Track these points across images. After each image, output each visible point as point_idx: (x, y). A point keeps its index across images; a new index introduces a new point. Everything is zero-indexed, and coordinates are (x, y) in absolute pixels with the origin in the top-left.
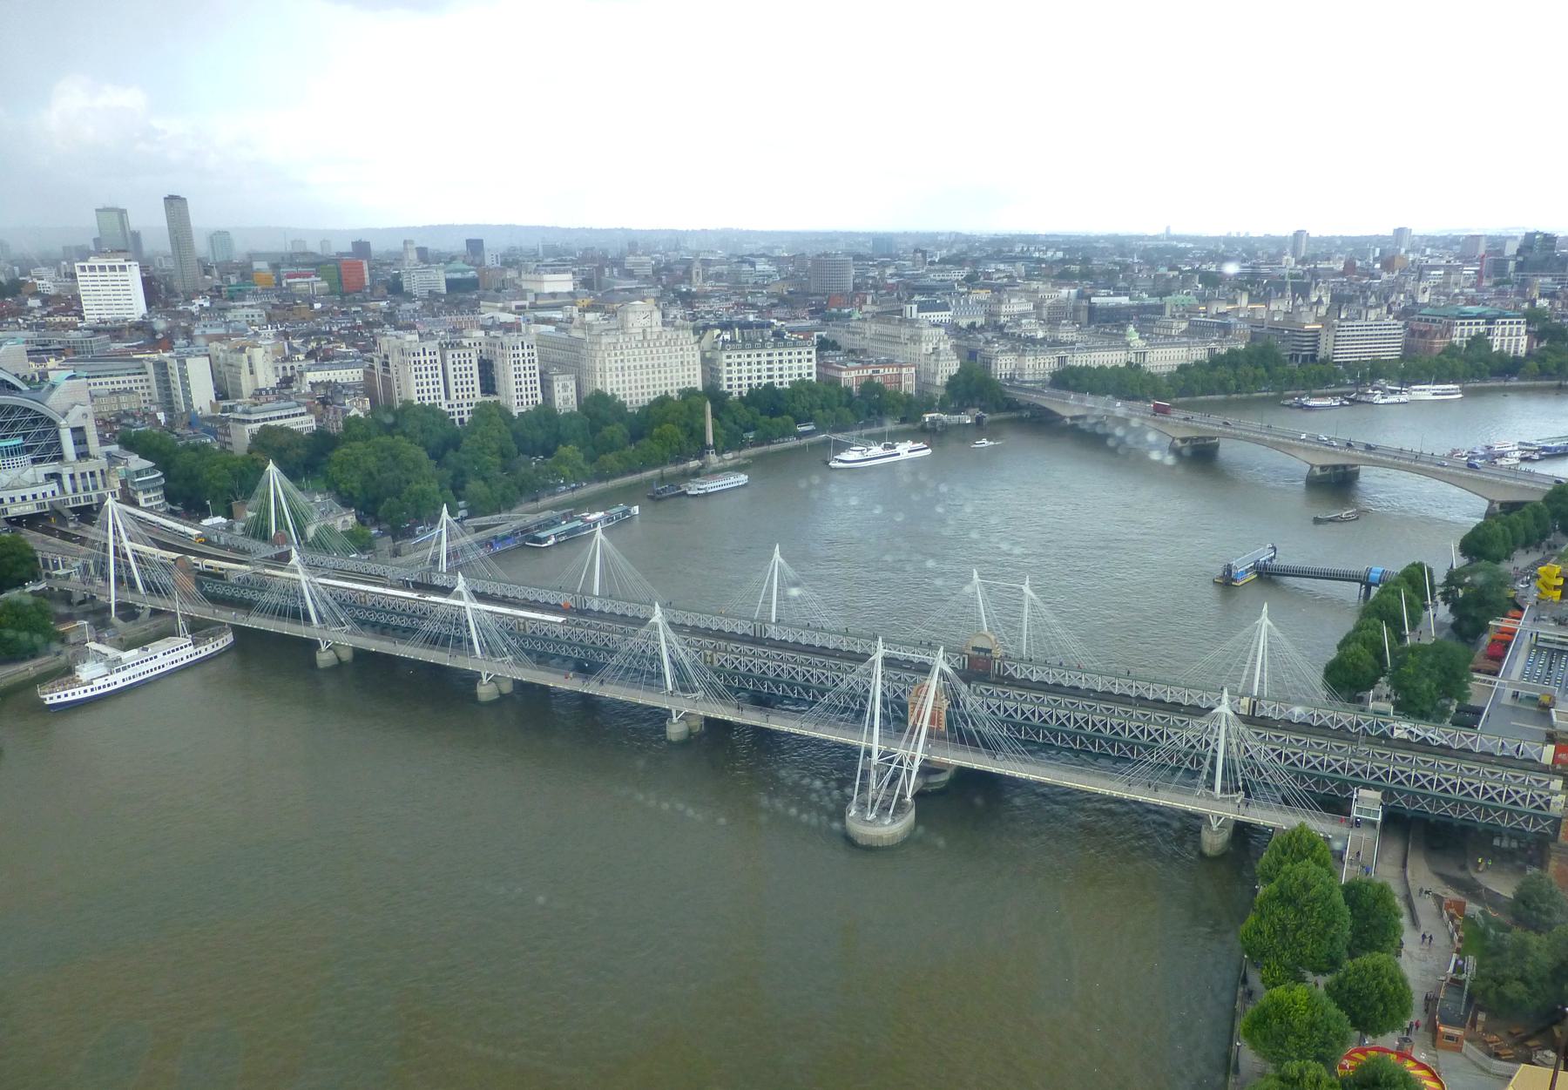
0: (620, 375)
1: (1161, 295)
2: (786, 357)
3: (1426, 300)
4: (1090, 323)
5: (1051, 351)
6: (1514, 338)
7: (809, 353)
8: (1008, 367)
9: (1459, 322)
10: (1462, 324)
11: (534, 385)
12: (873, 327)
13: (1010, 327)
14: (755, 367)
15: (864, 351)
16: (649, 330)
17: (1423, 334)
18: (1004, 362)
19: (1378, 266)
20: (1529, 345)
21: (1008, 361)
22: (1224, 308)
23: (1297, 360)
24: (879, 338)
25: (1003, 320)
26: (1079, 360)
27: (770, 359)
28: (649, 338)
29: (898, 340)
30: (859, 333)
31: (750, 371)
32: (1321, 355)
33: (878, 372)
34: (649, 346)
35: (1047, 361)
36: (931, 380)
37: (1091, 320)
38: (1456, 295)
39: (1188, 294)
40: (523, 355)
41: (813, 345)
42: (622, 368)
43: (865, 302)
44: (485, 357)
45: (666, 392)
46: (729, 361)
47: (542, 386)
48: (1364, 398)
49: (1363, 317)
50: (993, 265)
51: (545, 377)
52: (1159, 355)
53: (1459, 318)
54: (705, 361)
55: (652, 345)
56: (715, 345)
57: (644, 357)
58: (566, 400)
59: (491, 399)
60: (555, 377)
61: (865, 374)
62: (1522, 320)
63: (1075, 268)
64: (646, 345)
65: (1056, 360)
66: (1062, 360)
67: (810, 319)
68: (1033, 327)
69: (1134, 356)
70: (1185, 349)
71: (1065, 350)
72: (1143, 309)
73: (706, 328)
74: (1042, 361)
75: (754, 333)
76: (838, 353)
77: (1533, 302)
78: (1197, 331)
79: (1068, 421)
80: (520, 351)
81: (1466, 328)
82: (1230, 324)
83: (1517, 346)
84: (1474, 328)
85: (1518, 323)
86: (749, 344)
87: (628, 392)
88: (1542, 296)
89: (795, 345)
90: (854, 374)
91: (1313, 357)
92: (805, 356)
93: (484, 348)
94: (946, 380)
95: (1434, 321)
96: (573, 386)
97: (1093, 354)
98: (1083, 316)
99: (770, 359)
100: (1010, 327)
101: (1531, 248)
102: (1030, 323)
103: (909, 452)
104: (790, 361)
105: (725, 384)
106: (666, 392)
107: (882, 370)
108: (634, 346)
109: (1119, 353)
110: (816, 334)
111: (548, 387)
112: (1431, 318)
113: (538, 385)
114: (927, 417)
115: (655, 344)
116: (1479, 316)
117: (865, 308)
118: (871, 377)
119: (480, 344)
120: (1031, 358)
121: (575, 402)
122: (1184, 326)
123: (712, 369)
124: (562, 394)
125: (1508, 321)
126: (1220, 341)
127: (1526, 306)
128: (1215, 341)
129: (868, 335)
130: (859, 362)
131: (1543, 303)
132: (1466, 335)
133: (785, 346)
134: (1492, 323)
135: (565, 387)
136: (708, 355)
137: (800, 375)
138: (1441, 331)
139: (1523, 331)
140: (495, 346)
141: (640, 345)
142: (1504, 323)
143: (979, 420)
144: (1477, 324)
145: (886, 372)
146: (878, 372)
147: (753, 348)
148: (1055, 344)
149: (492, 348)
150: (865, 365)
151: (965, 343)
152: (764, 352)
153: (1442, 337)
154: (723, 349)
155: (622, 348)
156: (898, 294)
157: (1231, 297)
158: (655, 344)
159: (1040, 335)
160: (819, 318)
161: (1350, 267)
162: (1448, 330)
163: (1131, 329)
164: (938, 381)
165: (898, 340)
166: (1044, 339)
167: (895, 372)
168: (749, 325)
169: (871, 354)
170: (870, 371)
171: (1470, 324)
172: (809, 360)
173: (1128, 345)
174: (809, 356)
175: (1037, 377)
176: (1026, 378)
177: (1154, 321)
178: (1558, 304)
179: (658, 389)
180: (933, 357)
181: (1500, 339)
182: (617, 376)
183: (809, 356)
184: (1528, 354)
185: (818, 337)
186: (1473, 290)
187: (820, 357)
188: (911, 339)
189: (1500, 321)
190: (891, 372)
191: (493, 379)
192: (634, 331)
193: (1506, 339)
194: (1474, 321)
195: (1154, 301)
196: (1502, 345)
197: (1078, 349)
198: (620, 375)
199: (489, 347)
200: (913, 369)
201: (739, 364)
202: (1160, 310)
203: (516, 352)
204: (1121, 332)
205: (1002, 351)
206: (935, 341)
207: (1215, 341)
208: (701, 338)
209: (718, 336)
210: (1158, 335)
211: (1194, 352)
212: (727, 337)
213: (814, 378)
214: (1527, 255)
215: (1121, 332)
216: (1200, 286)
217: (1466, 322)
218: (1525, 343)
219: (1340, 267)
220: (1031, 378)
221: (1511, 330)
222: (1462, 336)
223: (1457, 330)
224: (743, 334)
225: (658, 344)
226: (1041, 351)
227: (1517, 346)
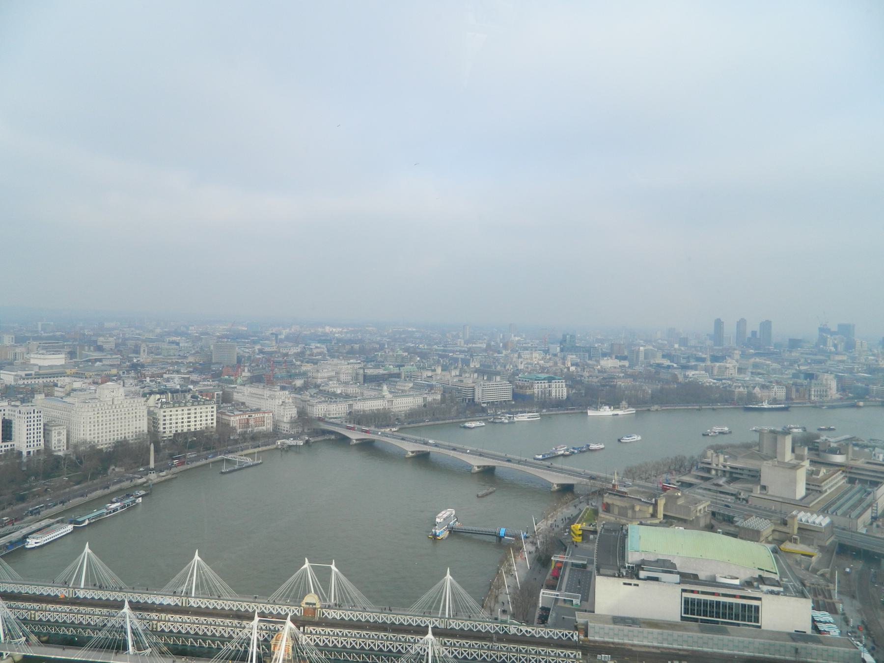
0: (96, 426)
1: (399, 366)
2: (198, 411)
3: (523, 367)
4: (365, 382)
5: (345, 401)
6: (561, 389)
7: (212, 408)
9: (536, 382)
10: (538, 383)
11: (39, 431)
12: (249, 389)
13: (323, 386)
14: (180, 417)
15: (243, 404)
16: (116, 399)
17: (522, 388)
18: (320, 408)
19: (501, 345)
20: (568, 392)
21: (323, 407)
22: (430, 374)
23: (466, 401)
24: (252, 395)
25: (319, 381)
26: (360, 406)
27: (189, 412)
28: (115, 403)
29: (263, 397)
30: (241, 393)
31: (177, 419)
32: (476, 400)
33: (251, 416)
34: (116, 407)
35: (343, 406)
36: (281, 419)
37: (365, 382)
38: (536, 364)
39: (413, 365)
40: (34, 417)
41: (215, 403)
42: (98, 421)
43: (244, 371)
44: (7, 418)
45: (125, 437)
46: (165, 414)
47: (44, 433)
48: (497, 421)
49: (494, 380)
50: (314, 344)
51: (46, 427)
52: (400, 402)
53: (536, 380)
54: (150, 413)
55: (117, 407)
56: (156, 405)
57: (112, 415)
58: (59, 441)
59: (9, 444)
60: (53, 428)
61: (244, 417)
62: (564, 381)
63: (357, 346)
64: (114, 407)
65: (347, 406)
66: (351, 406)
67: (213, 381)
68: (335, 385)
69: (387, 402)
70: (412, 398)
71: (352, 400)
72: (391, 375)
73: (151, 393)
74: (340, 407)
75: (180, 395)
76: (229, 405)
77: (568, 368)
78: (418, 387)
79: (355, 441)
80: (32, 415)
82: (433, 385)
83: (562, 392)
84: (543, 384)
85: (562, 382)
86: (177, 403)
87: (100, 435)
88: (572, 365)
89: (204, 404)
90: (238, 418)
91: (473, 399)
92: (210, 409)
93: (7, 412)
94: (289, 418)
95: (526, 381)
96: (65, 433)
97: (366, 402)
98: (361, 378)
99: (189, 412)
100: (323, 386)
101: (565, 341)
102: (334, 384)
104: (201, 413)
105: (161, 429)
106: (125, 437)
107: (253, 415)
108: (106, 408)
109: (379, 401)
110: (216, 393)
111: (48, 434)
112: (524, 379)
113: (42, 435)
114: (279, 442)
115: (119, 407)
116: (544, 379)
117: (244, 374)
118: (248, 419)
119: (4, 410)
120: (335, 405)
121: (65, 442)
122: (411, 385)
123: (154, 418)
124: (57, 438)
126: (429, 394)
127: (566, 370)
129: (246, 394)
130: (241, 411)
131: (573, 369)
133: (198, 405)
134: (551, 382)
135: (59, 434)
136: (152, 409)
137: (206, 424)
138: (528, 386)
139: (564, 386)
140: (14, 411)
141: (110, 408)
142: (556, 382)
143: (307, 442)
144: (544, 383)
145: (256, 416)
146: (251, 416)
147: (179, 406)
148: (347, 397)
149: (13, 413)
150: (244, 412)
151: (299, 396)
152: (186, 408)
154: (161, 407)
155: (98, 410)
156: (263, 366)
157: (433, 368)
158: (119, 407)
159: (339, 391)
160: (218, 381)
161: (489, 346)
162: (532, 386)
163: (385, 388)
164: (285, 420)
165: (263, 397)
166: (341, 394)
167: (261, 415)
168: (177, 391)
169: (247, 404)
170: (247, 416)
171: (541, 383)
172: (212, 412)
173: (384, 397)
174: (213, 410)
175: (337, 416)
176: (332, 416)
177: (396, 382)
178: (579, 370)
179: (119, 432)
180: (283, 407)
182: (94, 426)
183: (213, 410)
184: (568, 397)
185: (217, 394)
186: (543, 362)
187: (219, 408)
188: (270, 397)
189: (554, 381)
190: (259, 416)
191: (11, 431)
192: (107, 399)
193: (558, 389)
194: (543, 381)
195: (396, 370)
196: (556, 392)
197: (359, 400)
198: (96, 426)
199: (10, 413)
200: (271, 414)
201: (171, 415)
202: (398, 376)
203: (29, 416)
204: (380, 388)
205: (320, 402)
206: (283, 398)
207: (426, 394)
208: (148, 399)
209: (159, 400)
210: (399, 390)
212: (164, 400)
213: (215, 421)
214: (564, 344)
215: (380, 388)
216: (418, 359)
217: (539, 382)
218: (566, 391)
219: (484, 346)
220: (335, 416)
221: (559, 385)
222: (538, 388)
223: (536, 386)
224: (173, 396)
225: (121, 406)
226: (340, 401)
227: (562, 392)
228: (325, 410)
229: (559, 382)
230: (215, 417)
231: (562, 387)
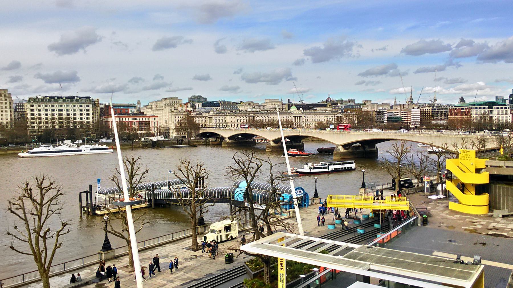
21: (221, 118)
46: (32, 108)
69: (293, 118)
71: (253, 114)
74: (239, 118)
103: (91, 150)
125: (500, 107)
128: (340, 113)
132: (478, 113)
142: (498, 108)
144: (484, 108)
153: (466, 115)
167: (147, 120)
181: (497, 116)
189: (496, 107)
207: (340, 113)
229: (502, 108)
230: (91, 116)
231: (506, 114)
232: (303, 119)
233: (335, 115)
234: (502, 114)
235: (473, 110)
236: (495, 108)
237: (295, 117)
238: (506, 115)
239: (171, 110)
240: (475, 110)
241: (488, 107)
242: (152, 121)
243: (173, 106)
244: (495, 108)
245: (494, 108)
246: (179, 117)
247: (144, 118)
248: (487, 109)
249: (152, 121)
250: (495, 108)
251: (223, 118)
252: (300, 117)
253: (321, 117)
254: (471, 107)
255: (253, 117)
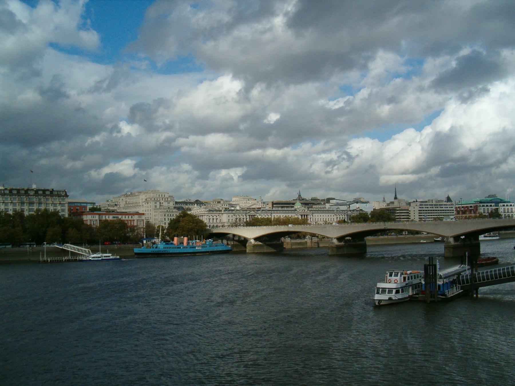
8: (215, 221)
9: (481, 204)
10: (483, 206)
71: (254, 211)
81: (486, 208)
84: (490, 208)
125: (505, 204)
134: (498, 206)
142: (504, 206)
144: (491, 206)
171: (487, 206)
189: (502, 204)
190: (127, 218)
194: (489, 204)
211: (338, 216)
217: (485, 204)
228: (218, 221)
229: (507, 206)
232: (311, 218)
233: (345, 213)
234: (511, 212)
235: (481, 208)
236: (501, 205)
237: (302, 215)
238: (512, 213)
239: (156, 206)
240: (482, 208)
241: (494, 204)
242: (137, 220)
243: (158, 201)
244: (501, 206)
245: (500, 205)
246: (169, 215)
247: (127, 216)
248: (494, 206)
249: (137, 220)
250: (501, 206)
251: (218, 216)
252: (307, 215)
253: (330, 216)
254: (478, 205)
255: (254, 215)
